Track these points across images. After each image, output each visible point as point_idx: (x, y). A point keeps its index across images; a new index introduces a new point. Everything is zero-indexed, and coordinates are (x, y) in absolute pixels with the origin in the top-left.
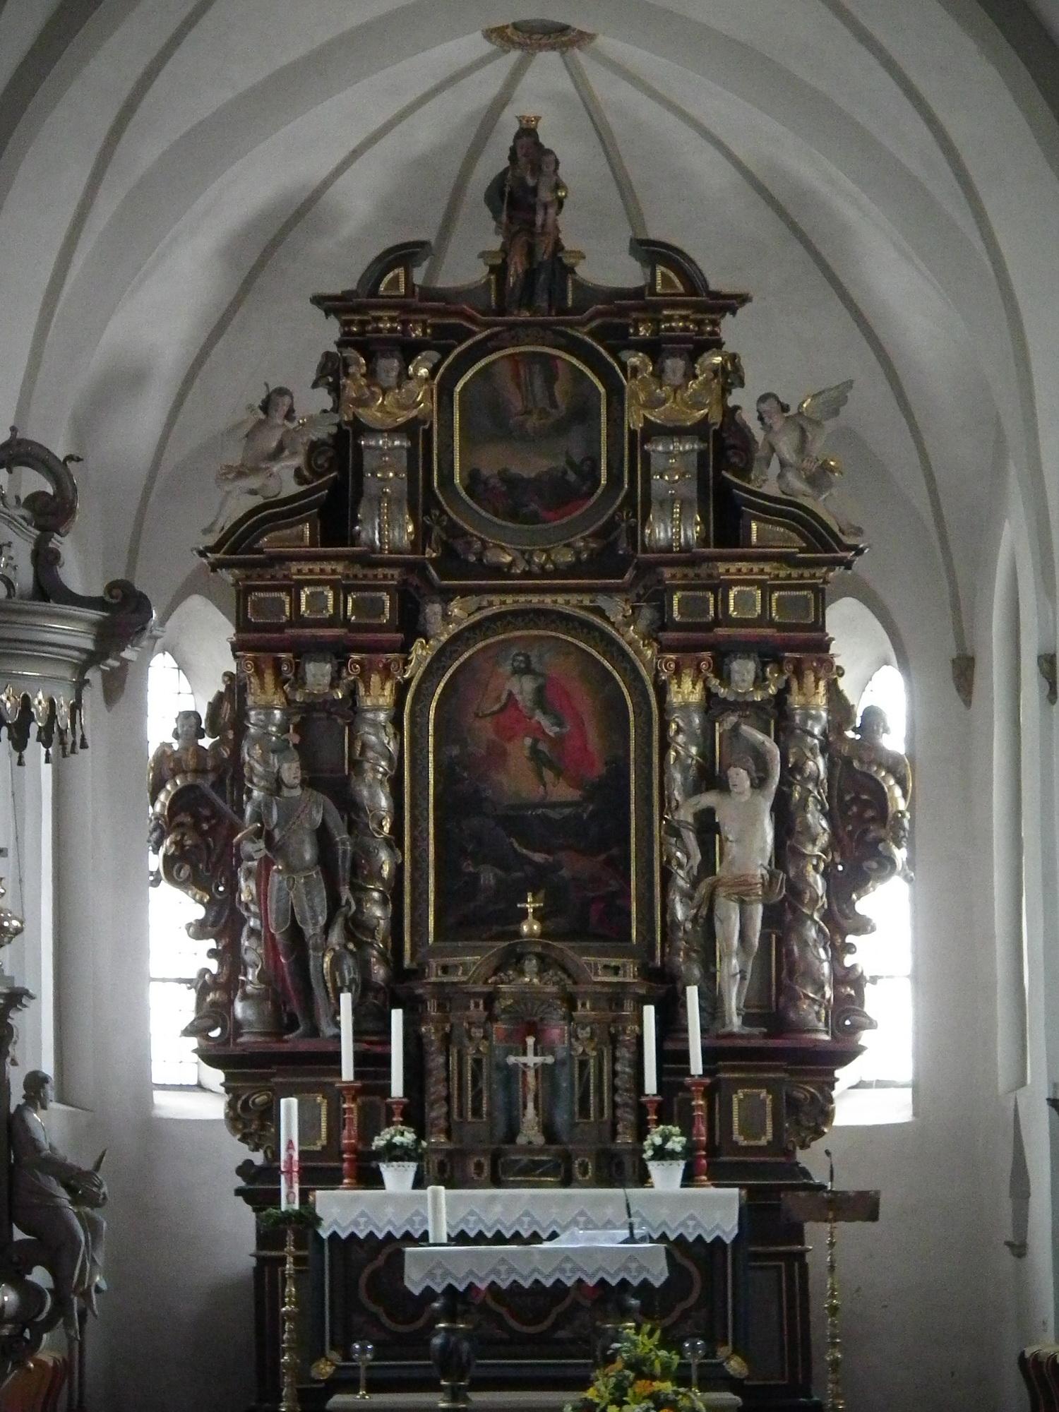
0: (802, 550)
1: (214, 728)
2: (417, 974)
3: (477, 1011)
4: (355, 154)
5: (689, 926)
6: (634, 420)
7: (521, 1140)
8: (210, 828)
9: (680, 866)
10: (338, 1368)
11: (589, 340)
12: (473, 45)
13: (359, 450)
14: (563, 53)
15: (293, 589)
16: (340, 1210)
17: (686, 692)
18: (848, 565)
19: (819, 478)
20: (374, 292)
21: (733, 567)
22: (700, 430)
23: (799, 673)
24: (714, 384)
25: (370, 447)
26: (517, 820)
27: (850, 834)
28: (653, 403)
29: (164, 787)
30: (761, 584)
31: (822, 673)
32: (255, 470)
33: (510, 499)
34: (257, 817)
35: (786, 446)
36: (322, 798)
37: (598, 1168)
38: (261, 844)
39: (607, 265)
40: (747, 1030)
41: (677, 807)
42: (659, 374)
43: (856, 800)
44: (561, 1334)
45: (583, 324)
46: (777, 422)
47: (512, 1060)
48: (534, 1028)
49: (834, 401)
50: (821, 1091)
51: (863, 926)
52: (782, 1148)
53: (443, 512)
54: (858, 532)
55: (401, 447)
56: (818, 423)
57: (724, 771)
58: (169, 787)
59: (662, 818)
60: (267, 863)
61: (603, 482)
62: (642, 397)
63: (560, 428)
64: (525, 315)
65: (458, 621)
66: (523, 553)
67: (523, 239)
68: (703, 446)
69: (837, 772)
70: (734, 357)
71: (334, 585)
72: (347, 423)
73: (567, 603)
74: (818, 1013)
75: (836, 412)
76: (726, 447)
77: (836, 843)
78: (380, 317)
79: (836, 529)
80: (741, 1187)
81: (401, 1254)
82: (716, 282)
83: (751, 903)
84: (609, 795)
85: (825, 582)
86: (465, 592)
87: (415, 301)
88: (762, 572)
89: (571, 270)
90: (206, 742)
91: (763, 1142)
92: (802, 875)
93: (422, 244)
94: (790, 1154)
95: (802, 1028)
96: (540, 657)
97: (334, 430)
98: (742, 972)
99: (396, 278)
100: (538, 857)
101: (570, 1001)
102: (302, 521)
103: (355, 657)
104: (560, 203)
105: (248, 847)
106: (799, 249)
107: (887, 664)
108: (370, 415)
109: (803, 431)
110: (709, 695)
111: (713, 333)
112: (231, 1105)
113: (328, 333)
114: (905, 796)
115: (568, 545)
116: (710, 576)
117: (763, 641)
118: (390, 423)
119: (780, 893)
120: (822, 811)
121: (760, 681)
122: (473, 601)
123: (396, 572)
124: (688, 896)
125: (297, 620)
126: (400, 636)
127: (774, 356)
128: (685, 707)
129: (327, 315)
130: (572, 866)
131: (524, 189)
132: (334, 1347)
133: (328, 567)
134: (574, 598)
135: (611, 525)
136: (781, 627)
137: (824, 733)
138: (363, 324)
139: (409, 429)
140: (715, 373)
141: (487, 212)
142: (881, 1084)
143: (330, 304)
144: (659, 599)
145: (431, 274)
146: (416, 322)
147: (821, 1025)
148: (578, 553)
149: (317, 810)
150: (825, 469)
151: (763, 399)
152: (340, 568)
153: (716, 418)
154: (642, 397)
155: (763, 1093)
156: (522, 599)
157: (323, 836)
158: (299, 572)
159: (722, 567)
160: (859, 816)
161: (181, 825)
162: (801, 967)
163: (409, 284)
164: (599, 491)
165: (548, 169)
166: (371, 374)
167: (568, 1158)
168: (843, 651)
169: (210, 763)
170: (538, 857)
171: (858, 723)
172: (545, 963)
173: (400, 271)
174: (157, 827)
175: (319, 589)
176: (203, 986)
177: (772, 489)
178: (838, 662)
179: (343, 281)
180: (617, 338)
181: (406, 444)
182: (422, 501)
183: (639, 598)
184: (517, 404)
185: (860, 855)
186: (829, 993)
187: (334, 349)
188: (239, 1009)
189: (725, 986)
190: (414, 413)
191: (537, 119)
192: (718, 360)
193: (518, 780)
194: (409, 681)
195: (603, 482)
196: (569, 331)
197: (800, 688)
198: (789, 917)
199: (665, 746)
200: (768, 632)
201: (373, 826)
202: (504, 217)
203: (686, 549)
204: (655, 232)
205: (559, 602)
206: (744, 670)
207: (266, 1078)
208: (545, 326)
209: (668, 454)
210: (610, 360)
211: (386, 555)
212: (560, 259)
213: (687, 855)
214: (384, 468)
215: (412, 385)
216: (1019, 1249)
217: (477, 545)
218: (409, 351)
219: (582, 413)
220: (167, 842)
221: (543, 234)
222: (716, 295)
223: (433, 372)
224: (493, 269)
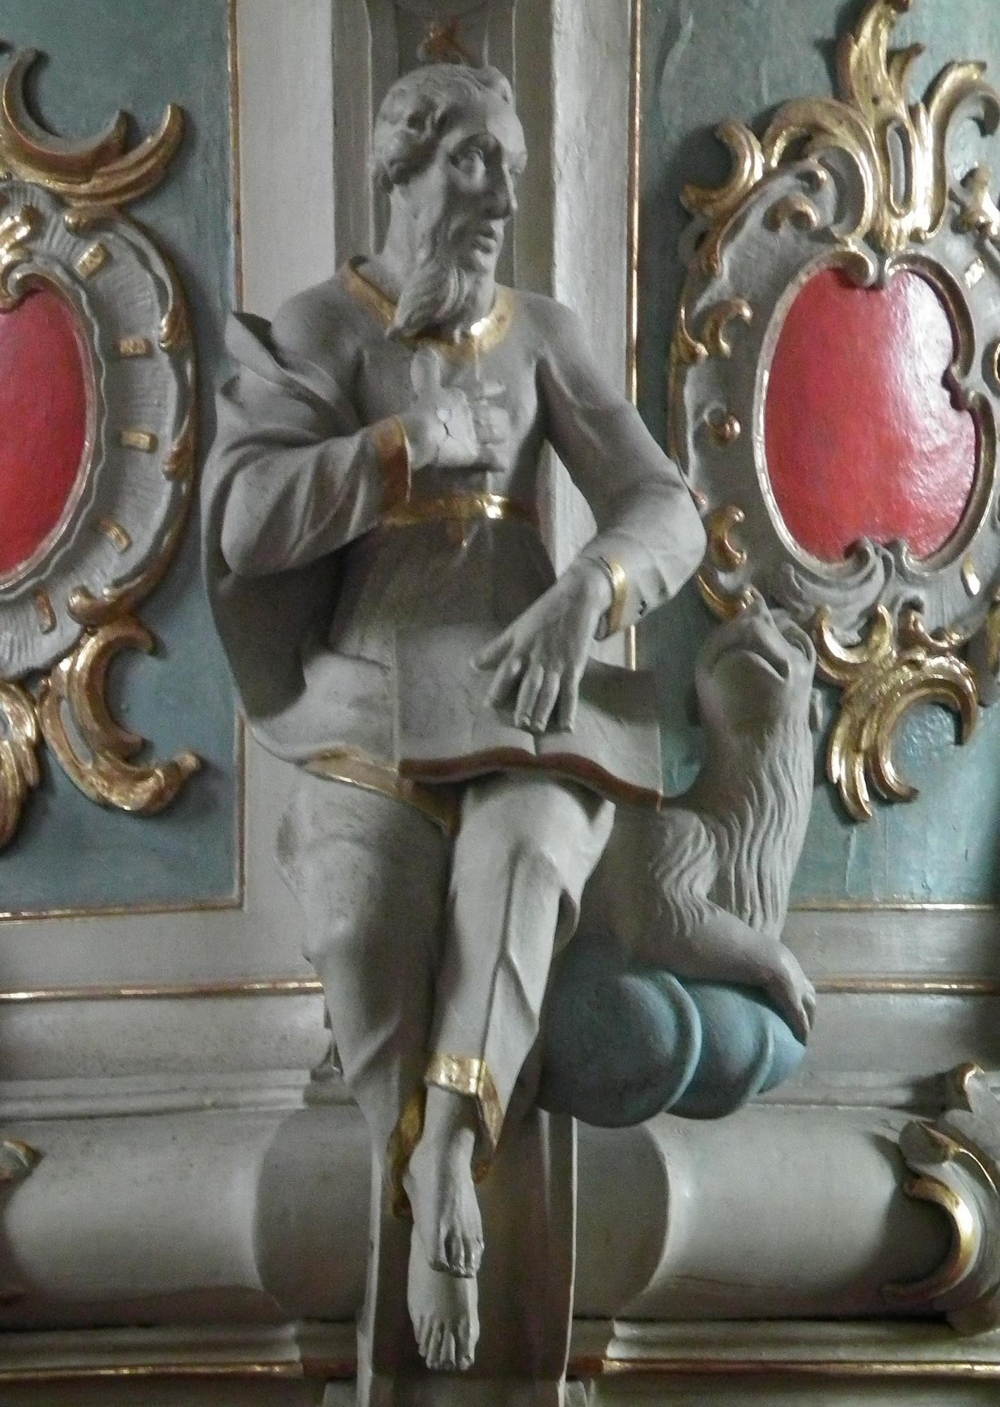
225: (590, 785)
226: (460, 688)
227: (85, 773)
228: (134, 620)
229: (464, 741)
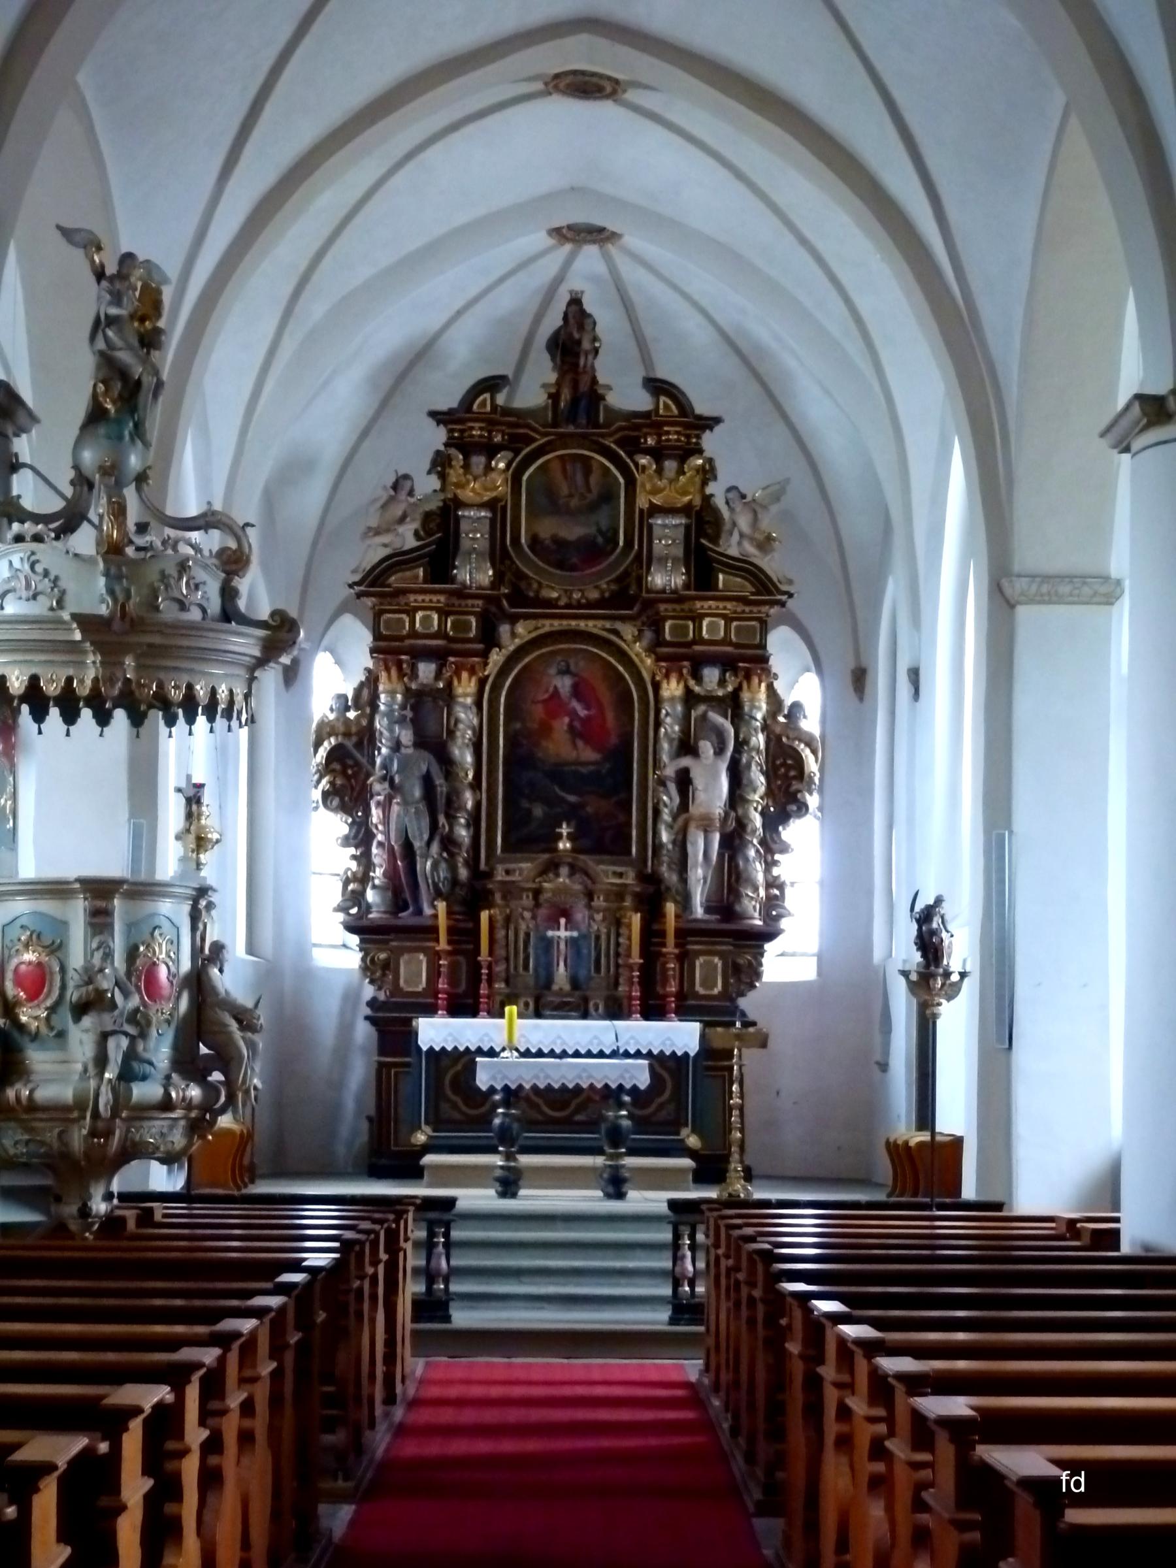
0: (753, 594)
1: (357, 705)
2: (489, 875)
3: (527, 901)
4: (459, 313)
5: (670, 846)
6: (642, 502)
7: (555, 987)
9: (666, 806)
10: (430, 1137)
11: (613, 445)
12: (539, 239)
13: (458, 519)
14: (601, 247)
15: (411, 613)
16: (435, 1032)
17: (672, 689)
18: (783, 604)
19: (765, 544)
20: (469, 409)
21: (707, 604)
22: (686, 510)
23: (748, 677)
24: (698, 480)
25: (464, 516)
26: (559, 774)
27: (780, 787)
28: (655, 491)
30: (723, 616)
31: (764, 677)
32: (388, 531)
33: (559, 555)
34: (385, 766)
35: (744, 522)
37: (606, 1007)
38: (386, 785)
39: (626, 394)
40: (707, 917)
41: (665, 766)
42: (660, 471)
43: (784, 764)
44: (578, 1118)
45: (611, 435)
46: (738, 507)
47: (550, 933)
48: (566, 913)
49: (777, 494)
50: (756, 959)
51: (785, 849)
52: (730, 997)
53: (513, 562)
54: (790, 582)
55: (485, 517)
56: (765, 507)
57: (696, 742)
59: (654, 773)
60: (389, 799)
61: (621, 544)
62: (648, 487)
63: (593, 507)
64: (571, 429)
65: (521, 637)
66: (566, 591)
67: (568, 377)
68: (688, 521)
69: (772, 744)
70: (710, 461)
71: (439, 610)
72: (450, 499)
73: (595, 626)
74: (754, 907)
75: (778, 499)
76: (703, 522)
77: (769, 793)
78: (475, 425)
79: (775, 580)
80: (700, 1021)
81: (474, 1063)
82: (701, 408)
83: (712, 831)
84: (620, 756)
85: (768, 616)
86: (527, 617)
87: (497, 417)
88: (725, 608)
89: (602, 398)
90: (352, 715)
91: (716, 991)
92: (746, 815)
93: (503, 378)
94: (733, 1000)
95: (742, 917)
96: (576, 664)
97: (441, 504)
98: (705, 879)
99: (485, 401)
100: (572, 798)
101: (590, 895)
102: (419, 566)
103: (452, 659)
104: (596, 351)
105: (377, 787)
106: (755, 387)
107: (808, 671)
108: (467, 495)
109: (755, 513)
110: (688, 691)
111: (697, 444)
112: (363, 959)
113: (437, 437)
114: (816, 761)
115: (597, 587)
116: (691, 611)
117: (725, 654)
118: (478, 500)
119: (731, 824)
120: (761, 771)
121: (722, 682)
122: (532, 623)
123: (480, 602)
124: (670, 827)
125: (414, 634)
126: (481, 646)
127: (736, 460)
128: (672, 699)
129: (438, 425)
130: (594, 806)
131: (571, 342)
132: (427, 1123)
133: (435, 598)
134: (600, 623)
135: (626, 574)
136: (737, 646)
137: (764, 719)
138: (462, 431)
139: (491, 505)
140: (698, 471)
141: (546, 357)
142: (793, 955)
143: (438, 417)
144: (656, 625)
145: (510, 397)
146: (498, 431)
147: (756, 915)
148: (602, 592)
149: (425, 762)
150: (769, 538)
151: (729, 490)
152: (442, 598)
153: (698, 502)
154: (648, 487)
155: (716, 960)
156: (565, 622)
158: (416, 601)
159: (698, 604)
160: (786, 775)
162: (744, 875)
163: (494, 407)
164: (618, 550)
165: (588, 327)
166: (466, 466)
167: (586, 1000)
168: (776, 663)
169: (354, 729)
170: (572, 798)
171: (786, 712)
172: (574, 869)
173: (487, 396)
174: (318, 771)
175: (428, 613)
177: (733, 551)
178: (774, 670)
179: (449, 400)
180: (633, 446)
181: (489, 515)
182: (498, 555)
183: (643, 624)
184: (564, 490)
185: (786, 798)
186: (762, 893)
187: (442, 448)
189: (693, 890)
190: (494, 494)
191: (582, 292)
192: (700, 462)
193: (560, 746)
194: (488, 677)
195: (621, 544)
196: (601, 440)
197: (749, 687)
198: (737, 842)
199: (658, 724)
200: (729, 649)
201: (462, 774)
202: (558, 359)
203: (675, 592)
204: (662, 373)
205: (590, 626)
206: (711, 675)
207: (386, 942)
208: (584, 436)
209: (665, 526)
210: (628, 461)
211: (473, 591)
212: (596, 391)
213: (670, 799)
214: (475, 531)
215: (493, 475)
216: (884, 1067)
217: (535, 586)
218: (491, 451)
219: (608, 497)
220: (324, 781)
221: (585, 372)
222: (700, 418)
223: (508, 466)
224: (550, 396)
225: (126, 1034)
226: (108, 1021)
227: (44, 1030)
228: (52, 1010)
229: (109, 1028)
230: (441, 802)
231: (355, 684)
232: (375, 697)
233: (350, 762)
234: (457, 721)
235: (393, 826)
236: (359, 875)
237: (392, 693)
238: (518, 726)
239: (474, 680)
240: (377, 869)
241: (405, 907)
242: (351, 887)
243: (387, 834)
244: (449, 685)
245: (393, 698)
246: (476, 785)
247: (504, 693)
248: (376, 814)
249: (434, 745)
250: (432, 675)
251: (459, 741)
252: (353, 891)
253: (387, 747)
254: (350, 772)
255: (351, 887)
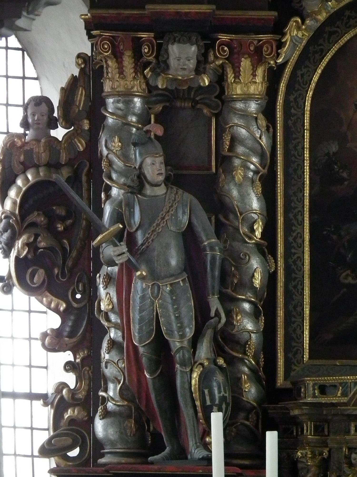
2: (292, 393)
8: (66, 229)
29: (14, 182)
34: (118, 217)
36: (188, 197)
38: (123, 248)
58: (19, 182)
60: (129, 269)
90: (59, 133)
103: (224, 37)
105: (109, 251)
149: (184, 210)
157: (189, 239)
161: (33, 225)
169: (63, 158)
176: (60, 402)
188: (100, 427)
194: (284, 65)
201: (244, 229)
220: (19, 243)
230: (212, 278)
231: (63, 82)
232: (96, 104)
233: (61, 211)
234: (234, 140)
235: (135, 315)
236: (81, 395)
237: (127, 96)
238: (334, 148)
239: (260, 71)
240: (111, 386)
241: (158, 447)
242: (68, 414)
243: (125, 327)
244: (220, 79)
245: (128, 103)
246: (267, 247)
247: (310, 94)
248: (106, 297)
249: (199, 179)
250: (192, 64)
251: (239, 174)
252: (72, 421)
253: (120, 187)
254: (60, 227)
255: (68, 414)
